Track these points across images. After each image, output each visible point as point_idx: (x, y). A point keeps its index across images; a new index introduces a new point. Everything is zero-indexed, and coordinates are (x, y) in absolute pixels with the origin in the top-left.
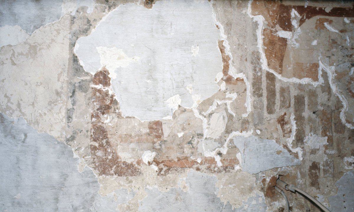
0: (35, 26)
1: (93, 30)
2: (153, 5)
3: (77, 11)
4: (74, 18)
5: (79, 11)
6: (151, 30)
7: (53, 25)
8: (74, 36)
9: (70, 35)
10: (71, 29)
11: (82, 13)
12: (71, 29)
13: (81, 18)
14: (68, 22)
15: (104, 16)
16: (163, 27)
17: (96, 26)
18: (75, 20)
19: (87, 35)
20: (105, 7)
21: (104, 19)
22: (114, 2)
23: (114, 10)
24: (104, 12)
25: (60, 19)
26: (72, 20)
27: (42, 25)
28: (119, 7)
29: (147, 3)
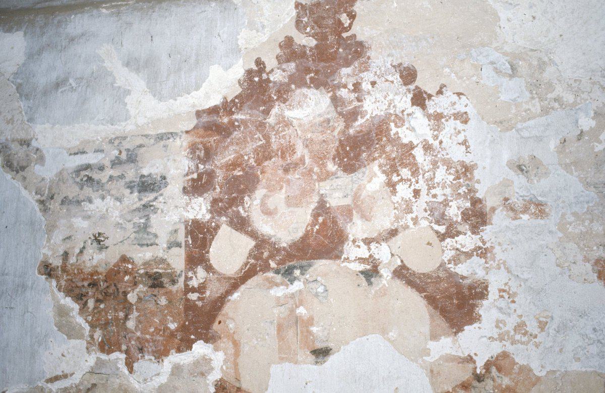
0: (21, 85)
1: (9, 176)
2: (44, 277)
3: (37, 149)
4: (28, 145)
5: (38, 152)
6: (6, 272)
7: (21, 112)
8: (3, 147)
9: (4, 141)
10: (13, 141)
11: (35, 156)
12: (13, 141)
13: (27, 156)
14: (22, 135)
15: (30, 192)
16: (8, 294)
17: (14, 182)
18: (25, 146)
19: (3, 167)
20: (44, 194)
21: (24, 193)
22: (50, 208)
23: (37, 209)
24: (36, 193)
25: (27, 123)
26: (25, 142)
27: (21, 96)
28: (42, 218)
29: (47, 266)
